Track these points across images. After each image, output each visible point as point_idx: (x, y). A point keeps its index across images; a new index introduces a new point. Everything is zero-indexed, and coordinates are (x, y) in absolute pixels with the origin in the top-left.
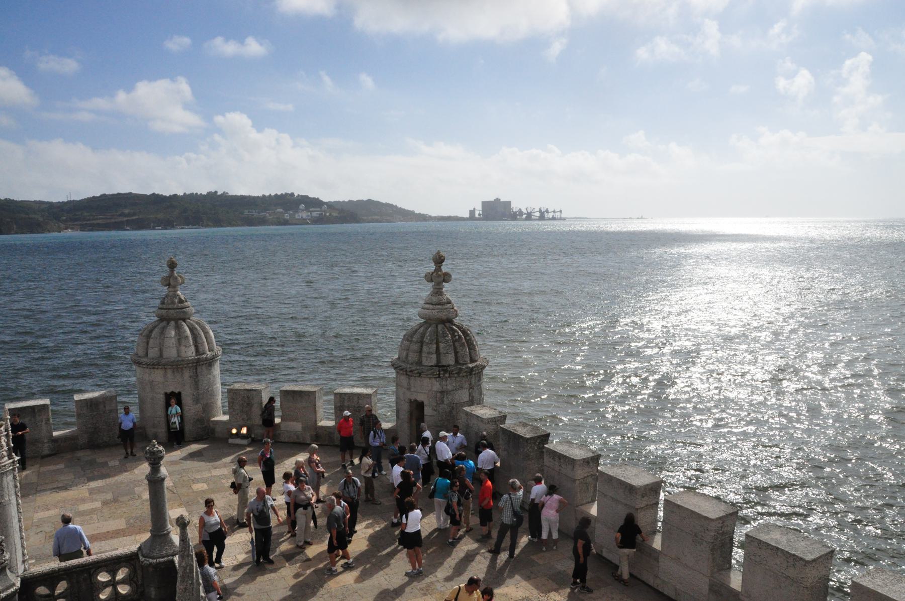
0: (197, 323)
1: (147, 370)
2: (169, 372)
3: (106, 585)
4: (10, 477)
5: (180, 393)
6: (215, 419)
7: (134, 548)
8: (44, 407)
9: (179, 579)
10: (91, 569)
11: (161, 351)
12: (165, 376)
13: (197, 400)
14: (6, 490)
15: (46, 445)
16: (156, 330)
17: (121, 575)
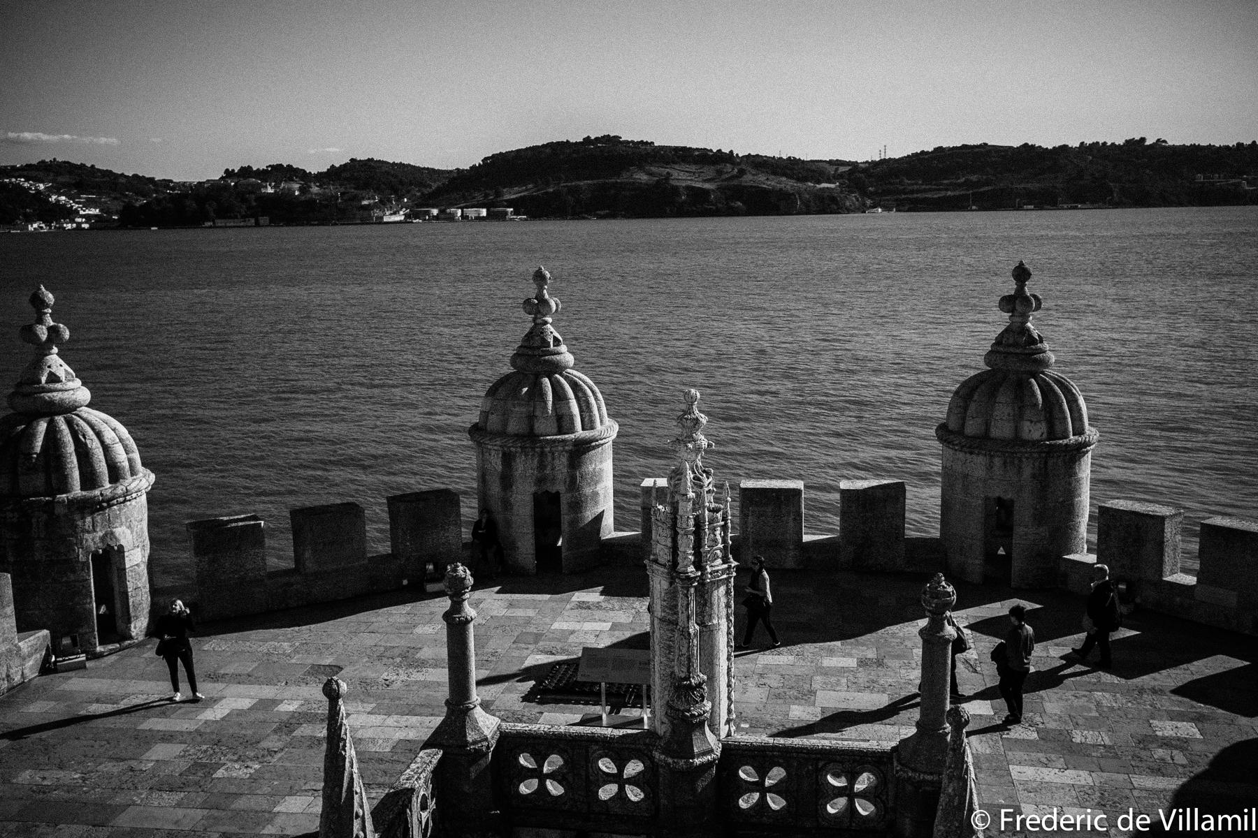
0: (1059, 382)
1: (961, 455)
2: (997, 461)
3: (839, 792)
4: (722, 589)
5: (1012, 501)
6: (1071, 557)
7: (888, 745)
8: (797, 492)
9: (939, 813)
10: (819, 759)
11: (987, 425)
12: (990, 467)
13: (1040, 518)
14: (715, 607)
15: (792, 553)
16: (983, 387)
17: (863, 782)
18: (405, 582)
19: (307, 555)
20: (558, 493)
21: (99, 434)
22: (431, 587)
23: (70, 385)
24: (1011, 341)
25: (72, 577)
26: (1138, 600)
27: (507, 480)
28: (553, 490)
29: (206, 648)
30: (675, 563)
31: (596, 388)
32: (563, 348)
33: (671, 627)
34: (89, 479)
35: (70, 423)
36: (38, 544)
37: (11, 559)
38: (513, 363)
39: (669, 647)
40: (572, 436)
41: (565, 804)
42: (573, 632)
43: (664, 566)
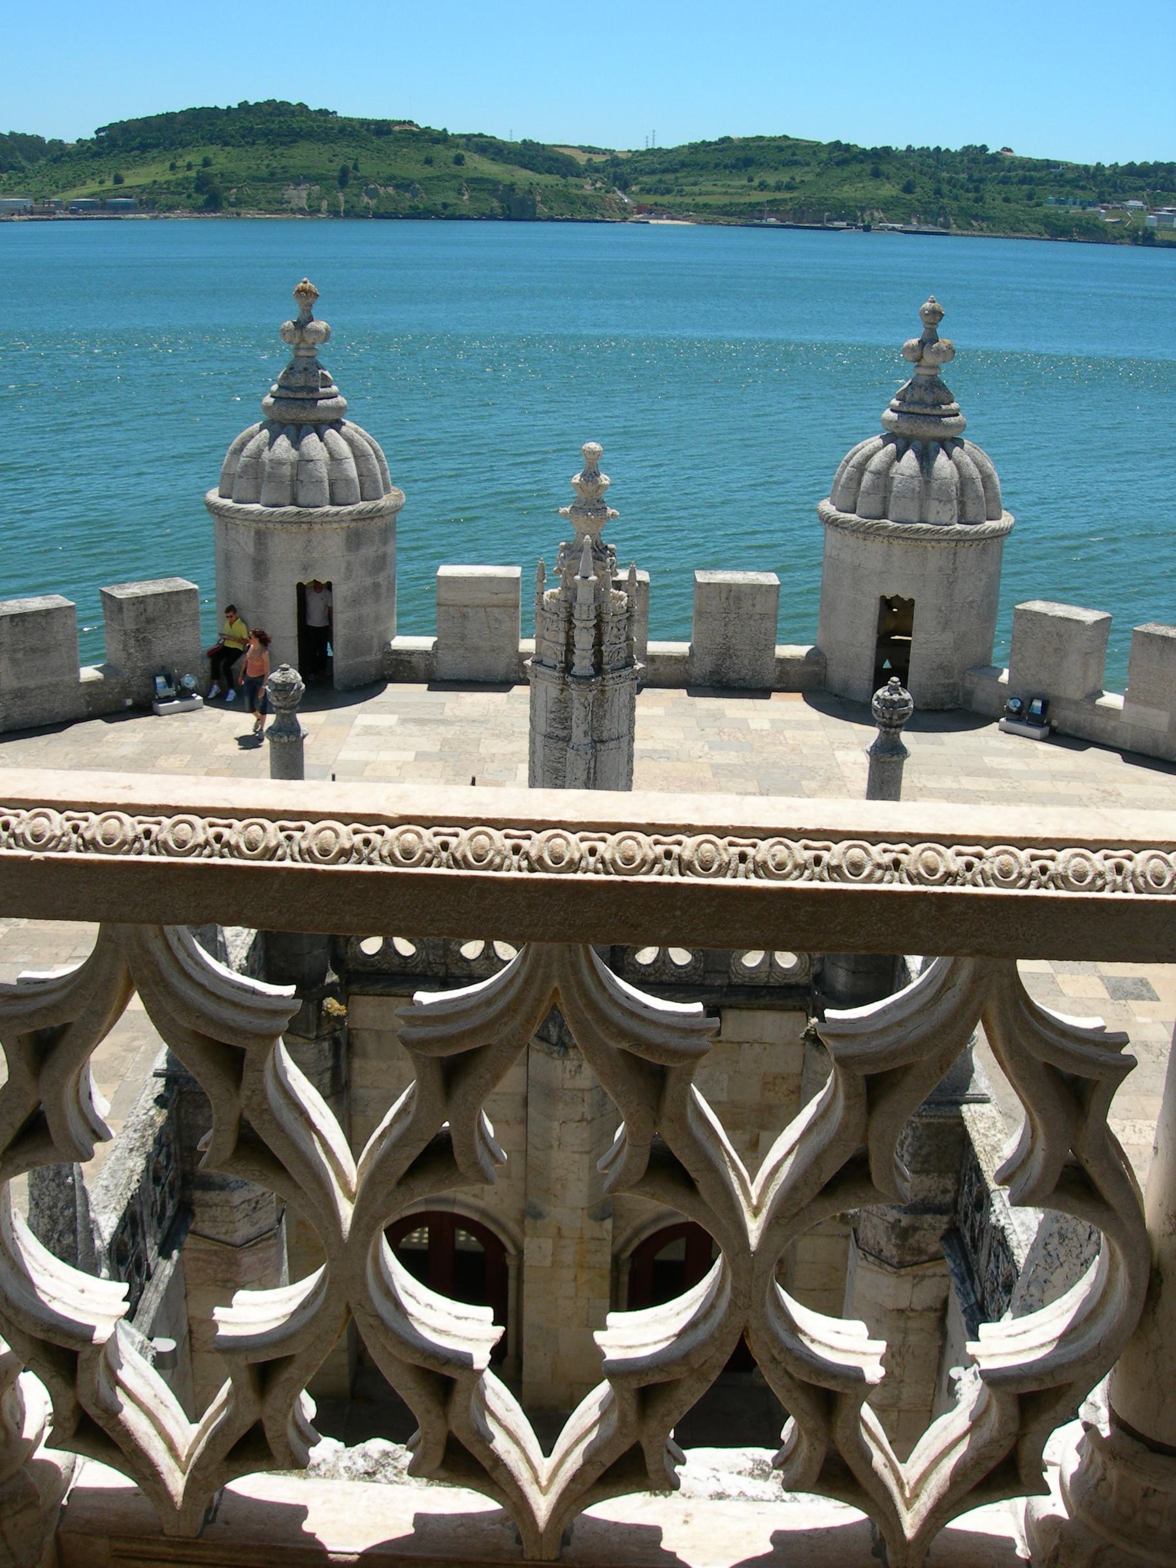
5: (912, 601)
18: (129, 702)
24: (916, 397)
26: (1055, 723)
30: (568, 667)
31: (377, 445)
32: (334, 388)
33: (561, 744)
39: (557, 770)
40: (350, 508)
41: (416, 966)
42: (366, 764)
43: (554, 667)
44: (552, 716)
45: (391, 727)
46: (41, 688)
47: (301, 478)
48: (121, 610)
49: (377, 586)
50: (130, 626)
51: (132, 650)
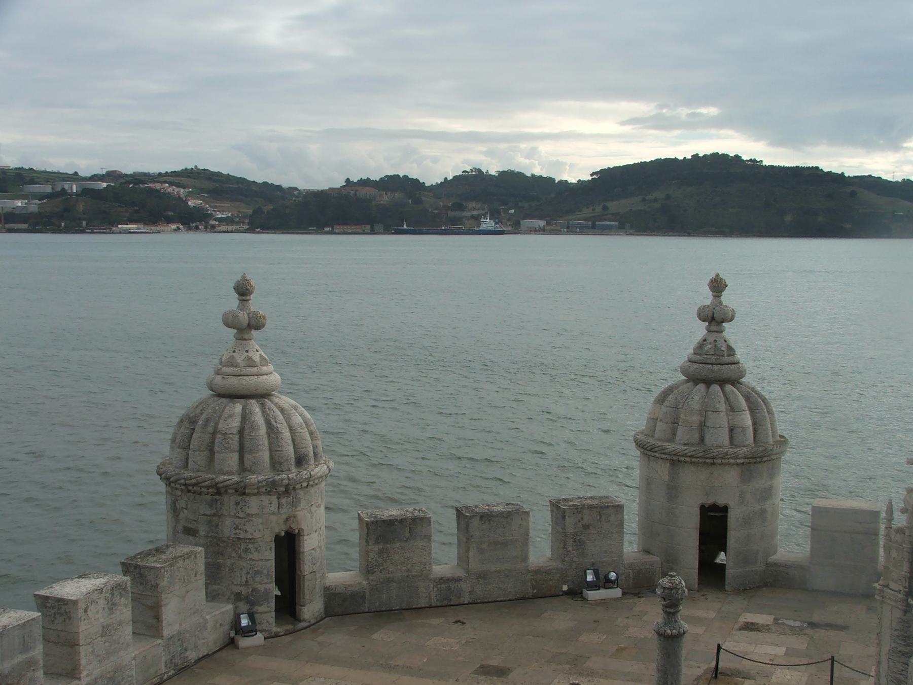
18: (565, 588)
19: (471, 554)
20: (725, 509)
21: (288, 418)
22: (592, 595)
23: (265, 369)
25: (256, 556)
27: (673, 491)
28: (721, 502)
29: (375, 636)
33: (903, 659)
34: (276, 464)
35: (263, 406)
36: (228, 522)
37: (202, 533)
38: (684, 371)
44: (896, 633)
45: (768, 625)
46: (499, 572)
47: (707, 424)
48: (564, 517)
49: (763, 512)
50: (570, 530)
51: (570, 549)
